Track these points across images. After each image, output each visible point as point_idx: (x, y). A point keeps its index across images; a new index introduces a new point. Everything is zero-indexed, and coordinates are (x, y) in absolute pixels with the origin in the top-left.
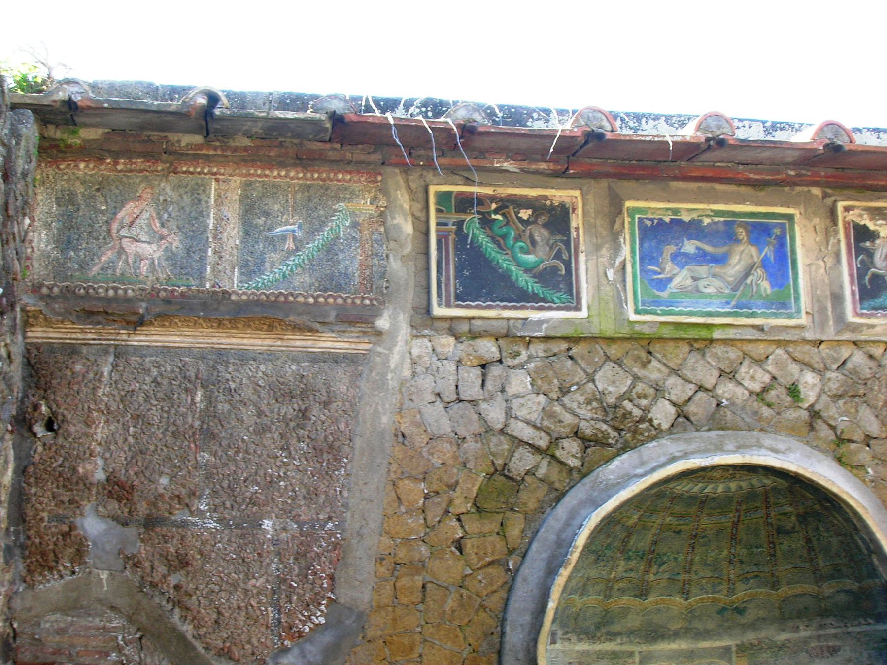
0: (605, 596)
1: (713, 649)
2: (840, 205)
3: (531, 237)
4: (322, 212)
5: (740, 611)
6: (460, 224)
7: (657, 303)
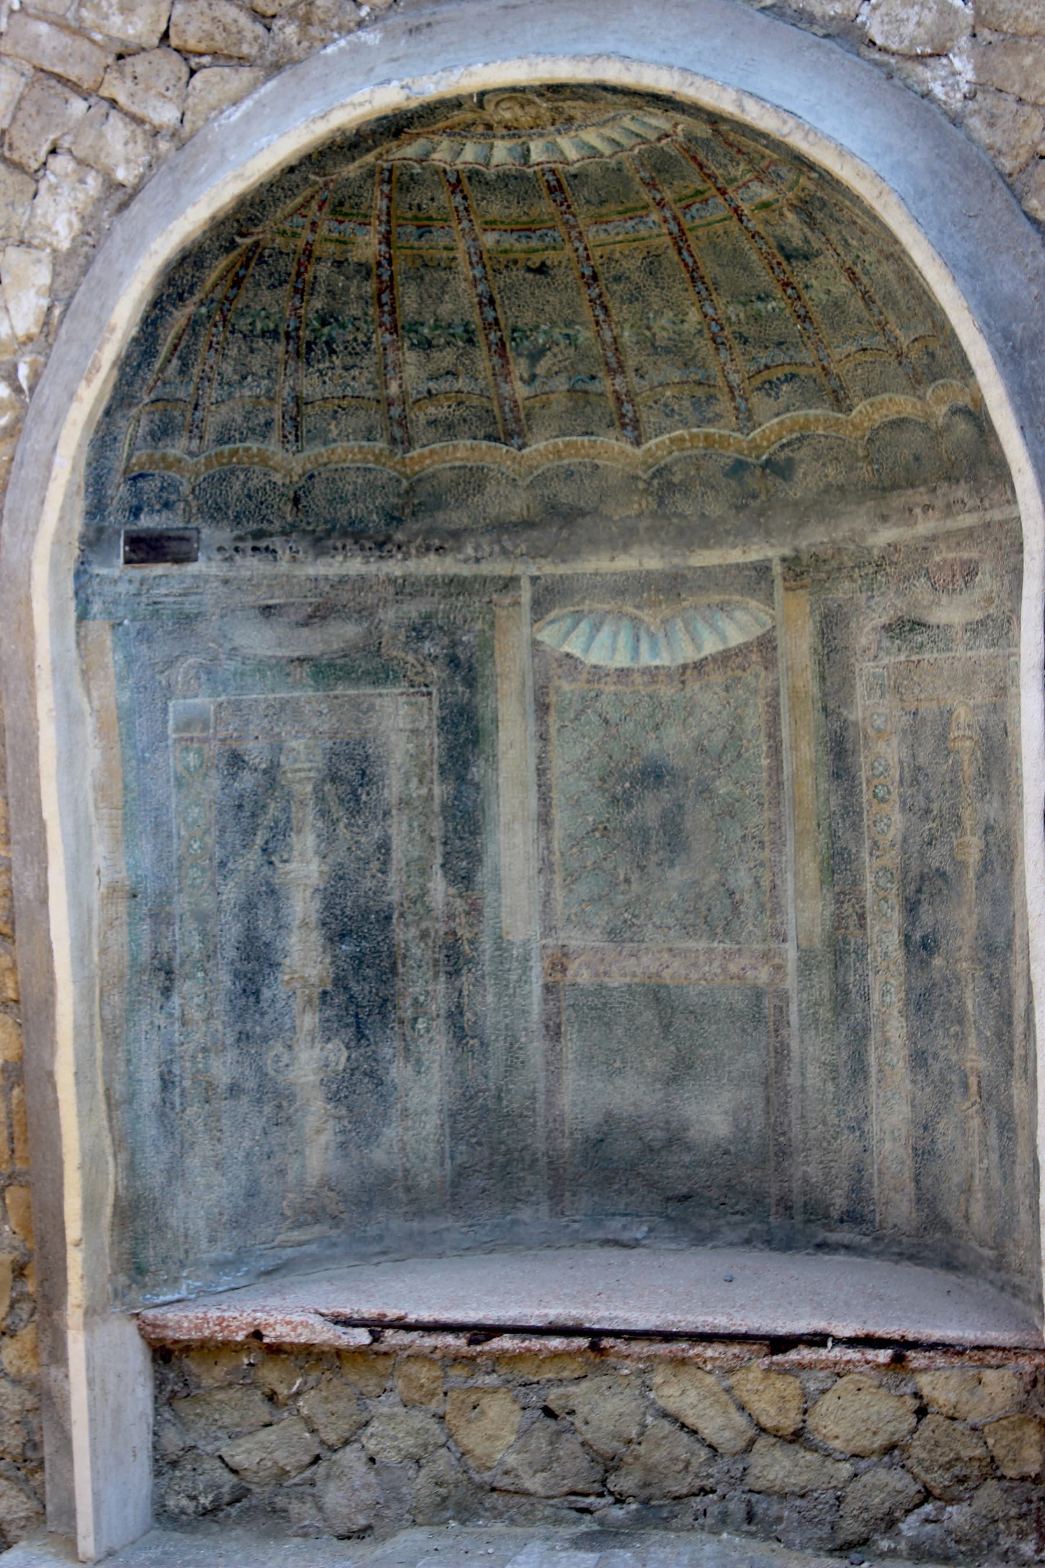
0: (393, 440)
1: (726, 569)
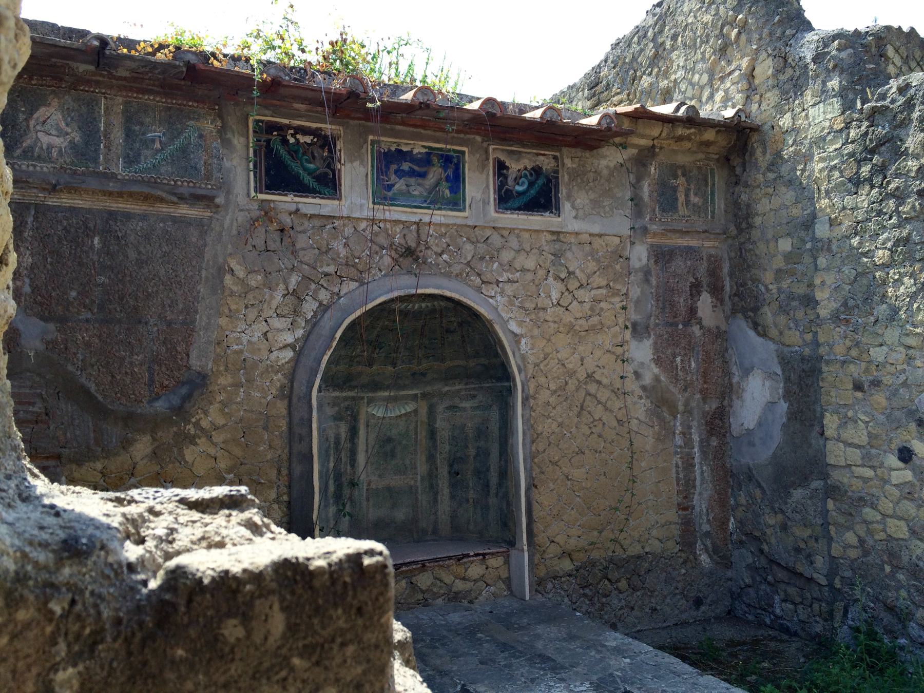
2: (491, 147)
3: (312, 153)
4: (179, 126)
5: (424, 375)
6: (268, 141)
7: (385, 199)
